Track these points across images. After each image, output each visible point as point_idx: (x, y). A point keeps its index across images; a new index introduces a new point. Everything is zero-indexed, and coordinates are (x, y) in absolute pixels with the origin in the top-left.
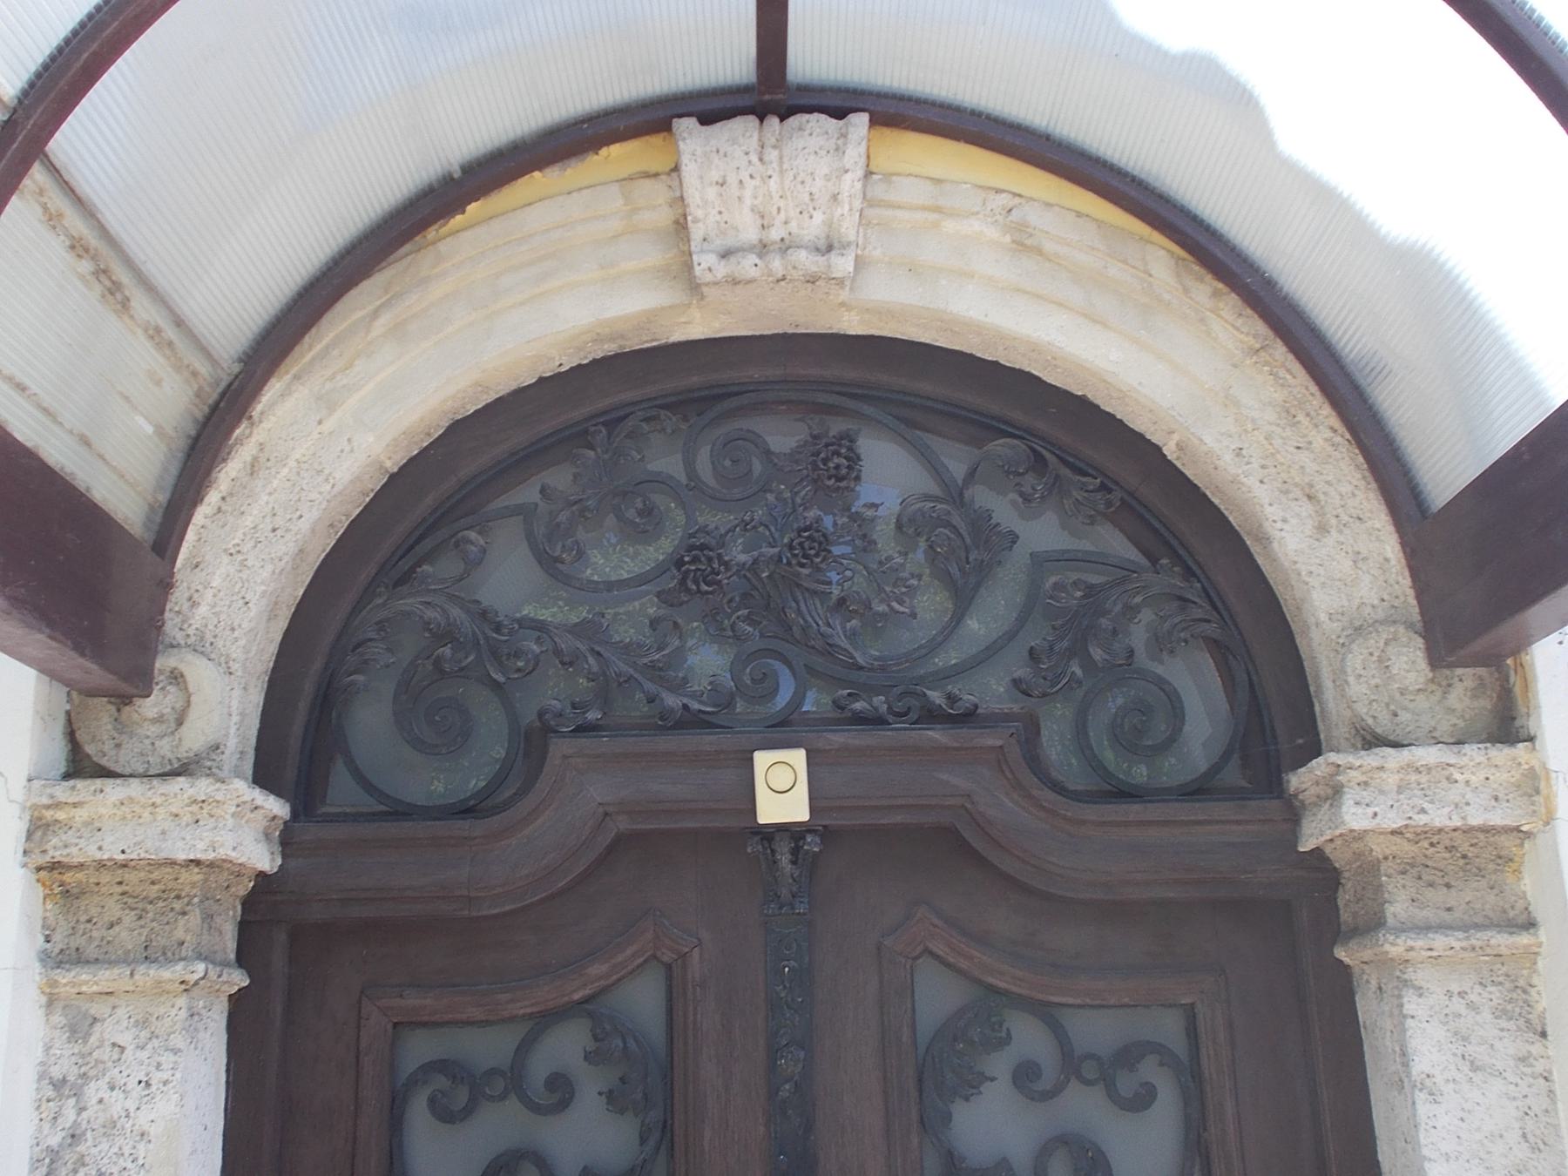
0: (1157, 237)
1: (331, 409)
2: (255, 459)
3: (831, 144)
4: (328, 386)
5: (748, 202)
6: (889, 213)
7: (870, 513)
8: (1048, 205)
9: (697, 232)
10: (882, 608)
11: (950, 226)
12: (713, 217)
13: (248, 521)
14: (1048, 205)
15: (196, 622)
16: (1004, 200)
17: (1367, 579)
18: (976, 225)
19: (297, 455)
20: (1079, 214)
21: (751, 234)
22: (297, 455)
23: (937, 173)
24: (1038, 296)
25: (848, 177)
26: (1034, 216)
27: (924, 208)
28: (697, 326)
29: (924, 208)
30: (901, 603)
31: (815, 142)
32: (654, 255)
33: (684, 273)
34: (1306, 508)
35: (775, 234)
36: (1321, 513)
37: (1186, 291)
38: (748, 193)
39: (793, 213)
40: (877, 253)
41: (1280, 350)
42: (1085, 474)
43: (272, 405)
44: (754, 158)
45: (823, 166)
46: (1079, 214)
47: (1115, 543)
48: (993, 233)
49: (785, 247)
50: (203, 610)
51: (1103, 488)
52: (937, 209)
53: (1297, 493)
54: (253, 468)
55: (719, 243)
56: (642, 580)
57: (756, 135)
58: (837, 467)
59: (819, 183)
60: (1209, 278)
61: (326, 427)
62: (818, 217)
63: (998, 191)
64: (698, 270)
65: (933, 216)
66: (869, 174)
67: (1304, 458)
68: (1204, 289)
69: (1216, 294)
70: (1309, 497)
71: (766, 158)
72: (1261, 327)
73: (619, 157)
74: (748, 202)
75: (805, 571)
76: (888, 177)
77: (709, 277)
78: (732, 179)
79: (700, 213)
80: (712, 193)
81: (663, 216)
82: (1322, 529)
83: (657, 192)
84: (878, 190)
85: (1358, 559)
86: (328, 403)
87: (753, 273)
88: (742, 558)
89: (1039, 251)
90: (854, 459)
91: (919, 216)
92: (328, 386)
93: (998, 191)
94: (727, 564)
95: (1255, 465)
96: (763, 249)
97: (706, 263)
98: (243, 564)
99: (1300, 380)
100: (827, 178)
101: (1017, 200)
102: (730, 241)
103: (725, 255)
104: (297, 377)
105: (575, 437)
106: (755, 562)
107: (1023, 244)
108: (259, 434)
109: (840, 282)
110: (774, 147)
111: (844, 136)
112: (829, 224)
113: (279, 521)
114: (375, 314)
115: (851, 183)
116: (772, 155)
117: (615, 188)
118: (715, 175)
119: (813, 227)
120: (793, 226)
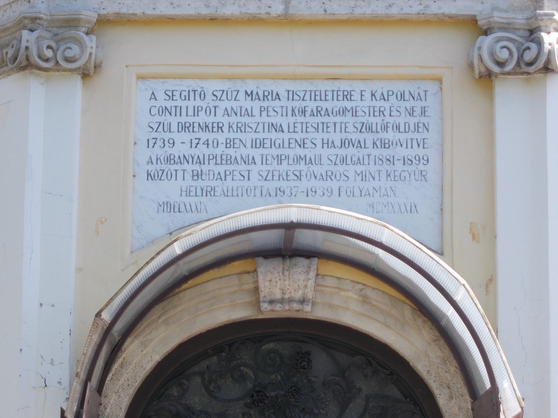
0: (408, 302)
1: (146, 347)
2: (122, 362)
3: (305, 270)
4: (144, 339)
5: (278, 287)
6: (322, 288)
7: (314, 379)
8: (374, 289)
9: (262, 295)
10: (316, 411)
11: (342, 293)
12: (267, 290)
13: (121, 382)
14: (374, 289)
15: (106, 414)
16: (360, 286)
17: (462, 414)
18: (350, 294)
19: (135, 361)
20: (384, 292)
21: (278, 295)
22: (135, 361)
23: (339, 275)
24: (370, 317)
25: (310, 281)
26: (369, 293)
27: (334, 287)
28: (260, 317)
29: (334, 287)
30: (323, 409)
31: (300, 270)
32: (247, 298)
33: (257, 304)
34: (447, 391)
35: (287, 296)
36: (451, 393)
37: (415, 320)
38: (278, 285)
39: (293, 291)
40: (319, 300)
41: (442, 342)
42: (385, 368)
43: (128, 346)
44: (281, 274)
45: (302, 277)
46: (384, 292)
47: (395, 392)
48: (356, 297)
49: (291, 301)
50: (108, 410)
51: (391, 374)
52: (339, 288)
53: (445, 386)
54: (122, 366)
55: (268, 298)
56: (239, 399)
57: (282, 266)
58: (304, 365)
59: (301, 282)
60: (422, 316)
61: (144, 353)
62: (300, 292)
63: (358, 283)
64: (262, 309)
65: (337, 290)
66: (317, 275)
67: (448, 375)
68: (420, 320)
69: (424, 322)
70: (448, 387)
71: (285, 274)
72: (437, 333)
73: (237, 266)
74: (278, 287)
75: (292, 400)
76: (324, 276)
77: (265, 310)
78: (274, 280)
79: (263, 289)
80: (267, 283)
81: (251, 286)
82: (451, 398)
83: (248, 278)
84: (320, 281)
85: (460, 408)
86: (144, 345)
87: (279, 309)
88: (273, 394)
89: (371, 303)
90: (309, 362)
91: (333, 290)
92: (144, 339)
93: (358, 283)
94: (267, 397)
95: (433, 376)
96: (282, 301)
97: (265, 306)
98: (119, 396)
99: (447, 351)
100: (304, 281)
101: (364, 287)
102: (272, 297)
103: (271, 302)
104: (135, 337)
105: (218, 350)
106: (277, 396)
107: (365, 300)
108: (124, 355)
109: (307, 312)
110: (287, 270)
111: (309, 267)
112: (304, 293)
113: (130, 383)
114: (159, 317)
115: (311, 283)
116: (287, 273)
117: (236, 277)
118: (268, 278)
119: (298, 295)
120: (292, 295)
